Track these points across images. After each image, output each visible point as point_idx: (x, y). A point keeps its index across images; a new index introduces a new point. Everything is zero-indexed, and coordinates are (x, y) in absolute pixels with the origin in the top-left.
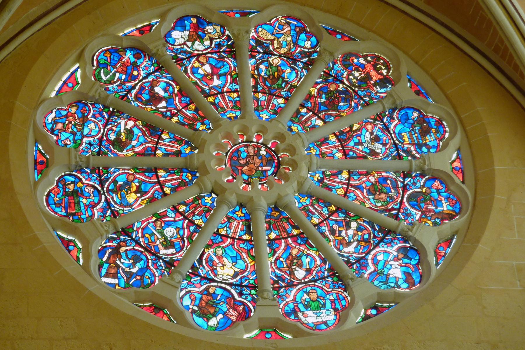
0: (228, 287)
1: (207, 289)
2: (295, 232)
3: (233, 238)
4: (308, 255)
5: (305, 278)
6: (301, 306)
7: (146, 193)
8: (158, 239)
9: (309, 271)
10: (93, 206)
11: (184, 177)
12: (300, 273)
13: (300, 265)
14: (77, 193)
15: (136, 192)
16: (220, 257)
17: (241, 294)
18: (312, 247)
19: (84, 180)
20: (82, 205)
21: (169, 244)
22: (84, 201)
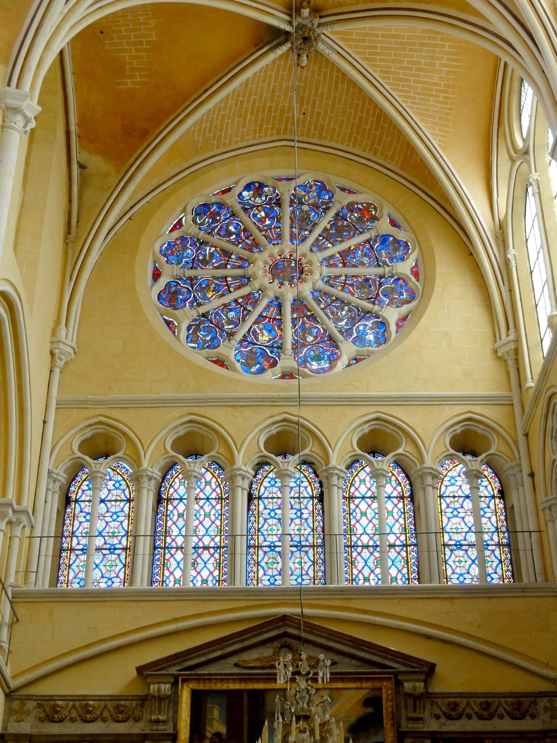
0: (265, 348)
1: (251, 350)
2: (309, 313)
3: (270, 318)
4: (316, 327)
5: (312, 342)
6: (309, 359)
7: (219, 291)
8: (224, 319)
9: (316, 338)
10: (186, 300)
11: (243, 282)
12: (310, 339)
13: (311, 334)
14: (177, 293)
15: (213, 291)
16: (261, 330)
17: (272, 352)
18: (318, 322)
19: (182, 285)
20: (179, 300)
21: (230, 322)
22: (181, 297)
